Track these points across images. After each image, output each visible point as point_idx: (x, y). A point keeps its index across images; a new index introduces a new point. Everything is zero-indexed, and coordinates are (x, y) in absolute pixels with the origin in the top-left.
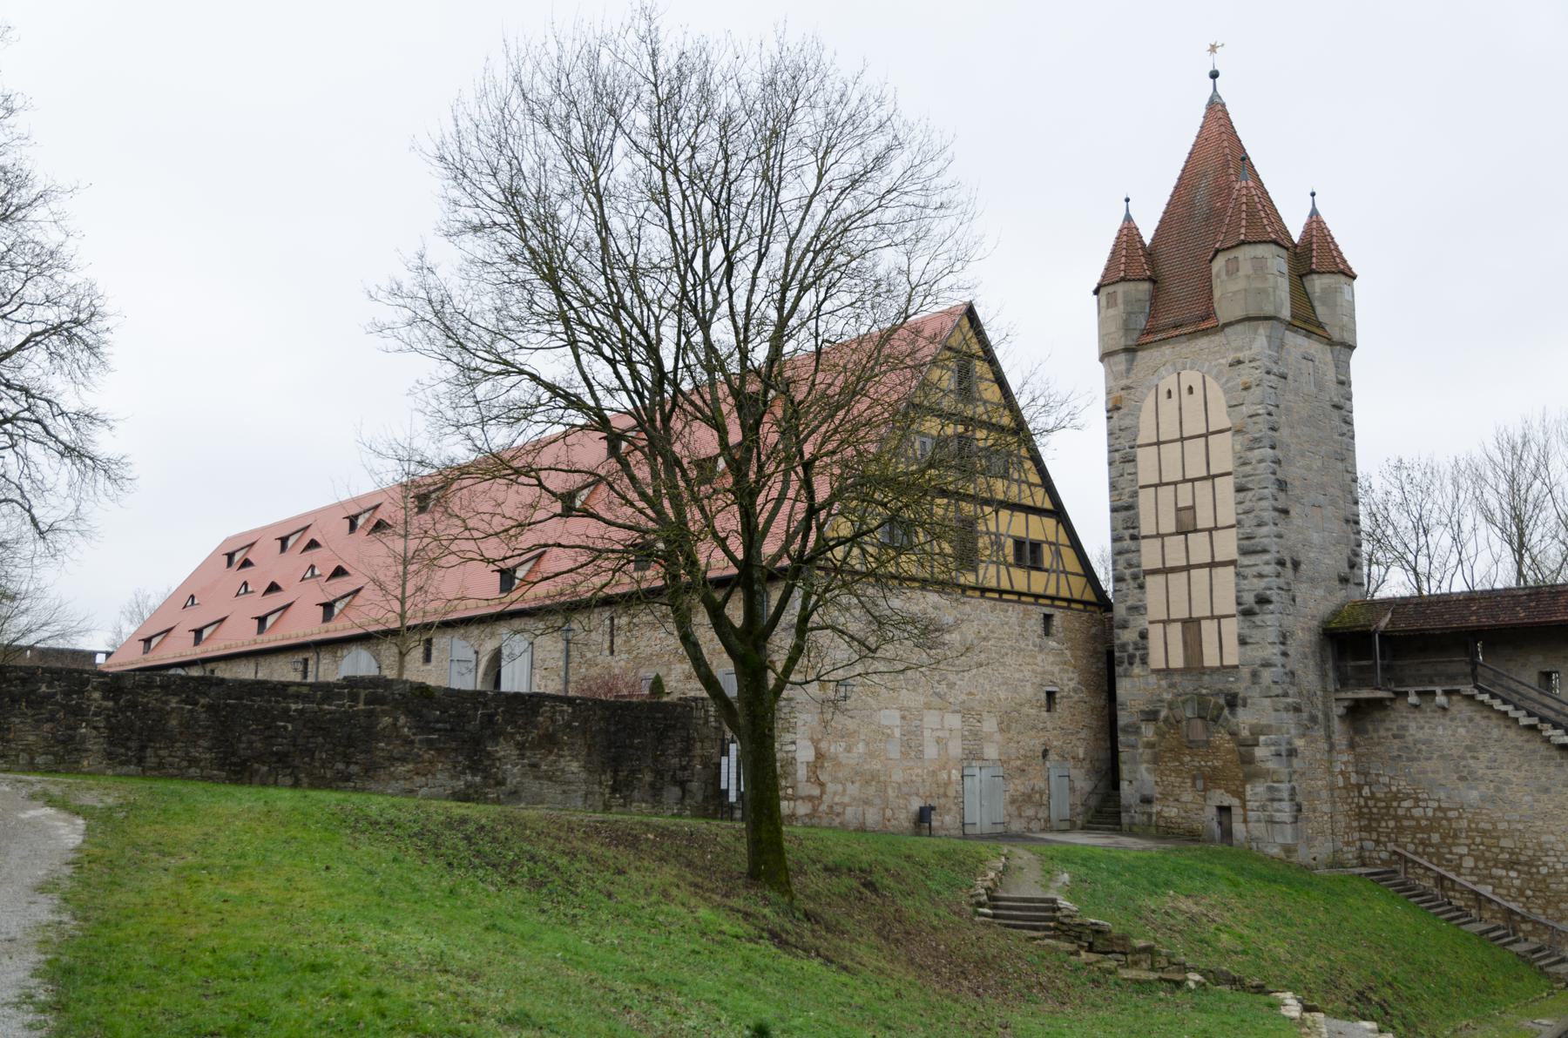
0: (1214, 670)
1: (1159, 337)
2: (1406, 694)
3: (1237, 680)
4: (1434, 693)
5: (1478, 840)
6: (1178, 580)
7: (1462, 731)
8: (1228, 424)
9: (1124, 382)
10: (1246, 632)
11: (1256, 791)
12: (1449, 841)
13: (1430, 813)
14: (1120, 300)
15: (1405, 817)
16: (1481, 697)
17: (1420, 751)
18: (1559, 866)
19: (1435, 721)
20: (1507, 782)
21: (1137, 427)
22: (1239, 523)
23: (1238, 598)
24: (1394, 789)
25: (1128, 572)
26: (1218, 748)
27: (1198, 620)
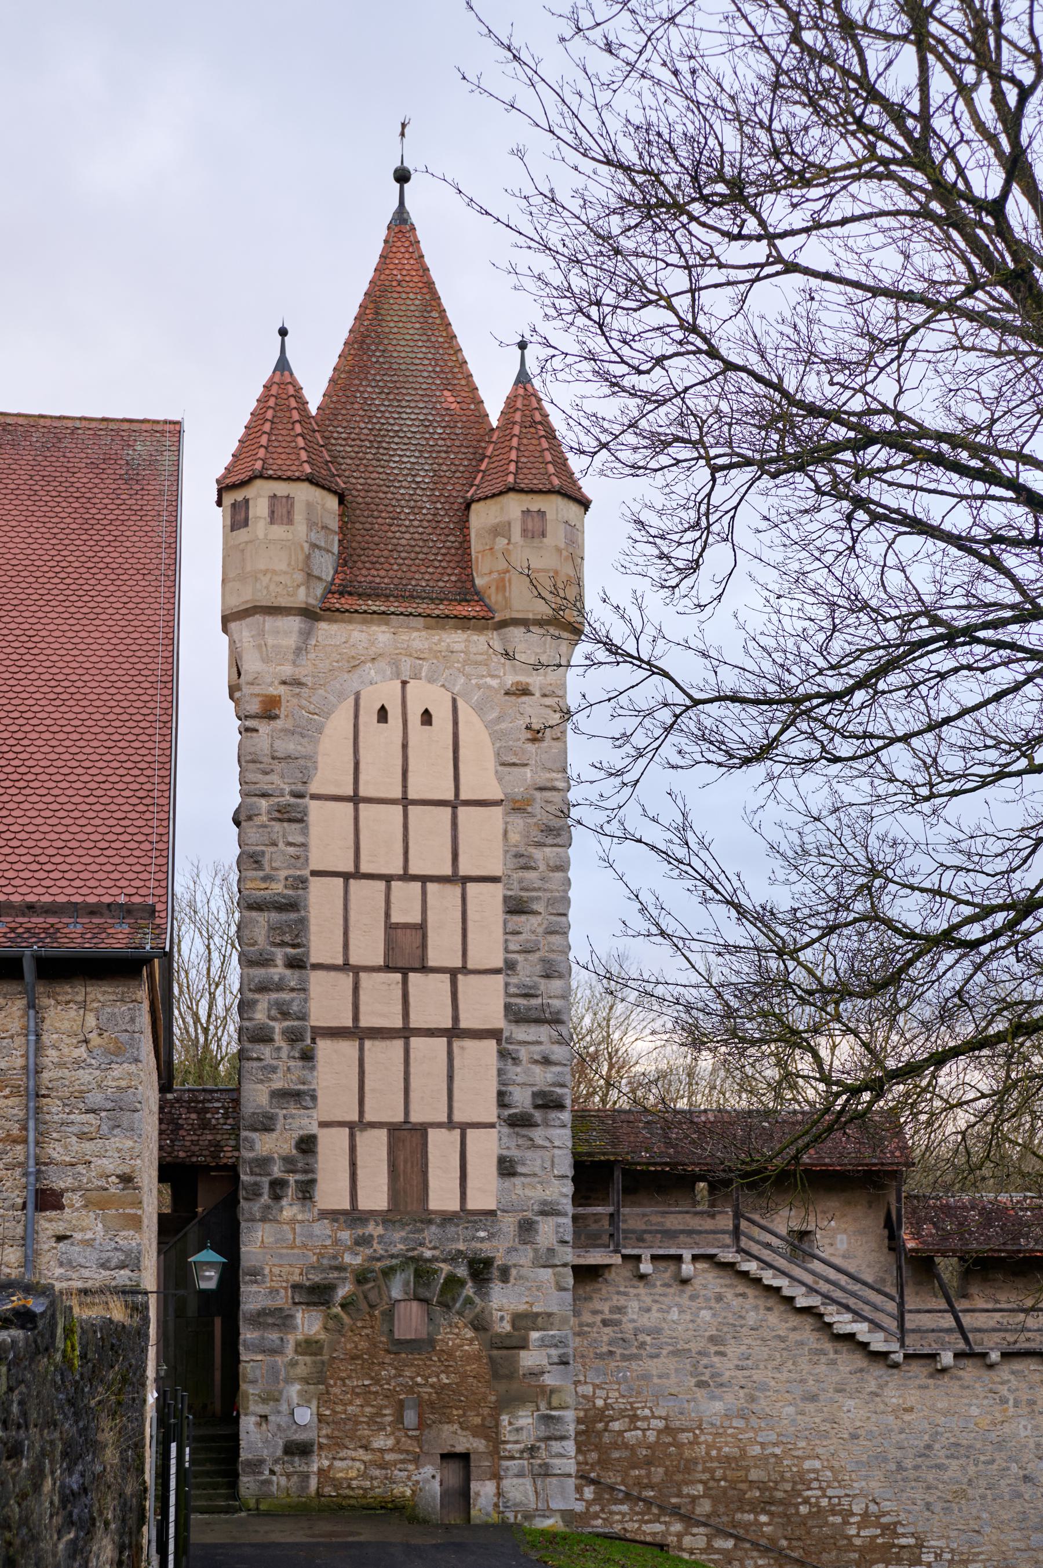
0: (448, 1218)
1: (374, 606)
2: (638, 1258)
3: (491, 1236)
4: (679, 1258)
5: (719, 1473)
6: (384, 1055)
7: (706, 1314)
8: (495, 793)
9: (287, 670)
10: (514, 1153)
11: (522, 1424)
12: (678, 1477)
13: (652, 1436)
14: (299, 517)
15: (615, 1446)
16: (745, 1267)
17: (642, 1345)
18: (824, 1502)
19: (667, 1300)
20: (764, 1388)
21: (311, 758)
22: (510, 966)
23: (501, 1094)
24: (600, 1403)
25: (278, 1027)
26: (450, 1354)
27: (422, 1130)
